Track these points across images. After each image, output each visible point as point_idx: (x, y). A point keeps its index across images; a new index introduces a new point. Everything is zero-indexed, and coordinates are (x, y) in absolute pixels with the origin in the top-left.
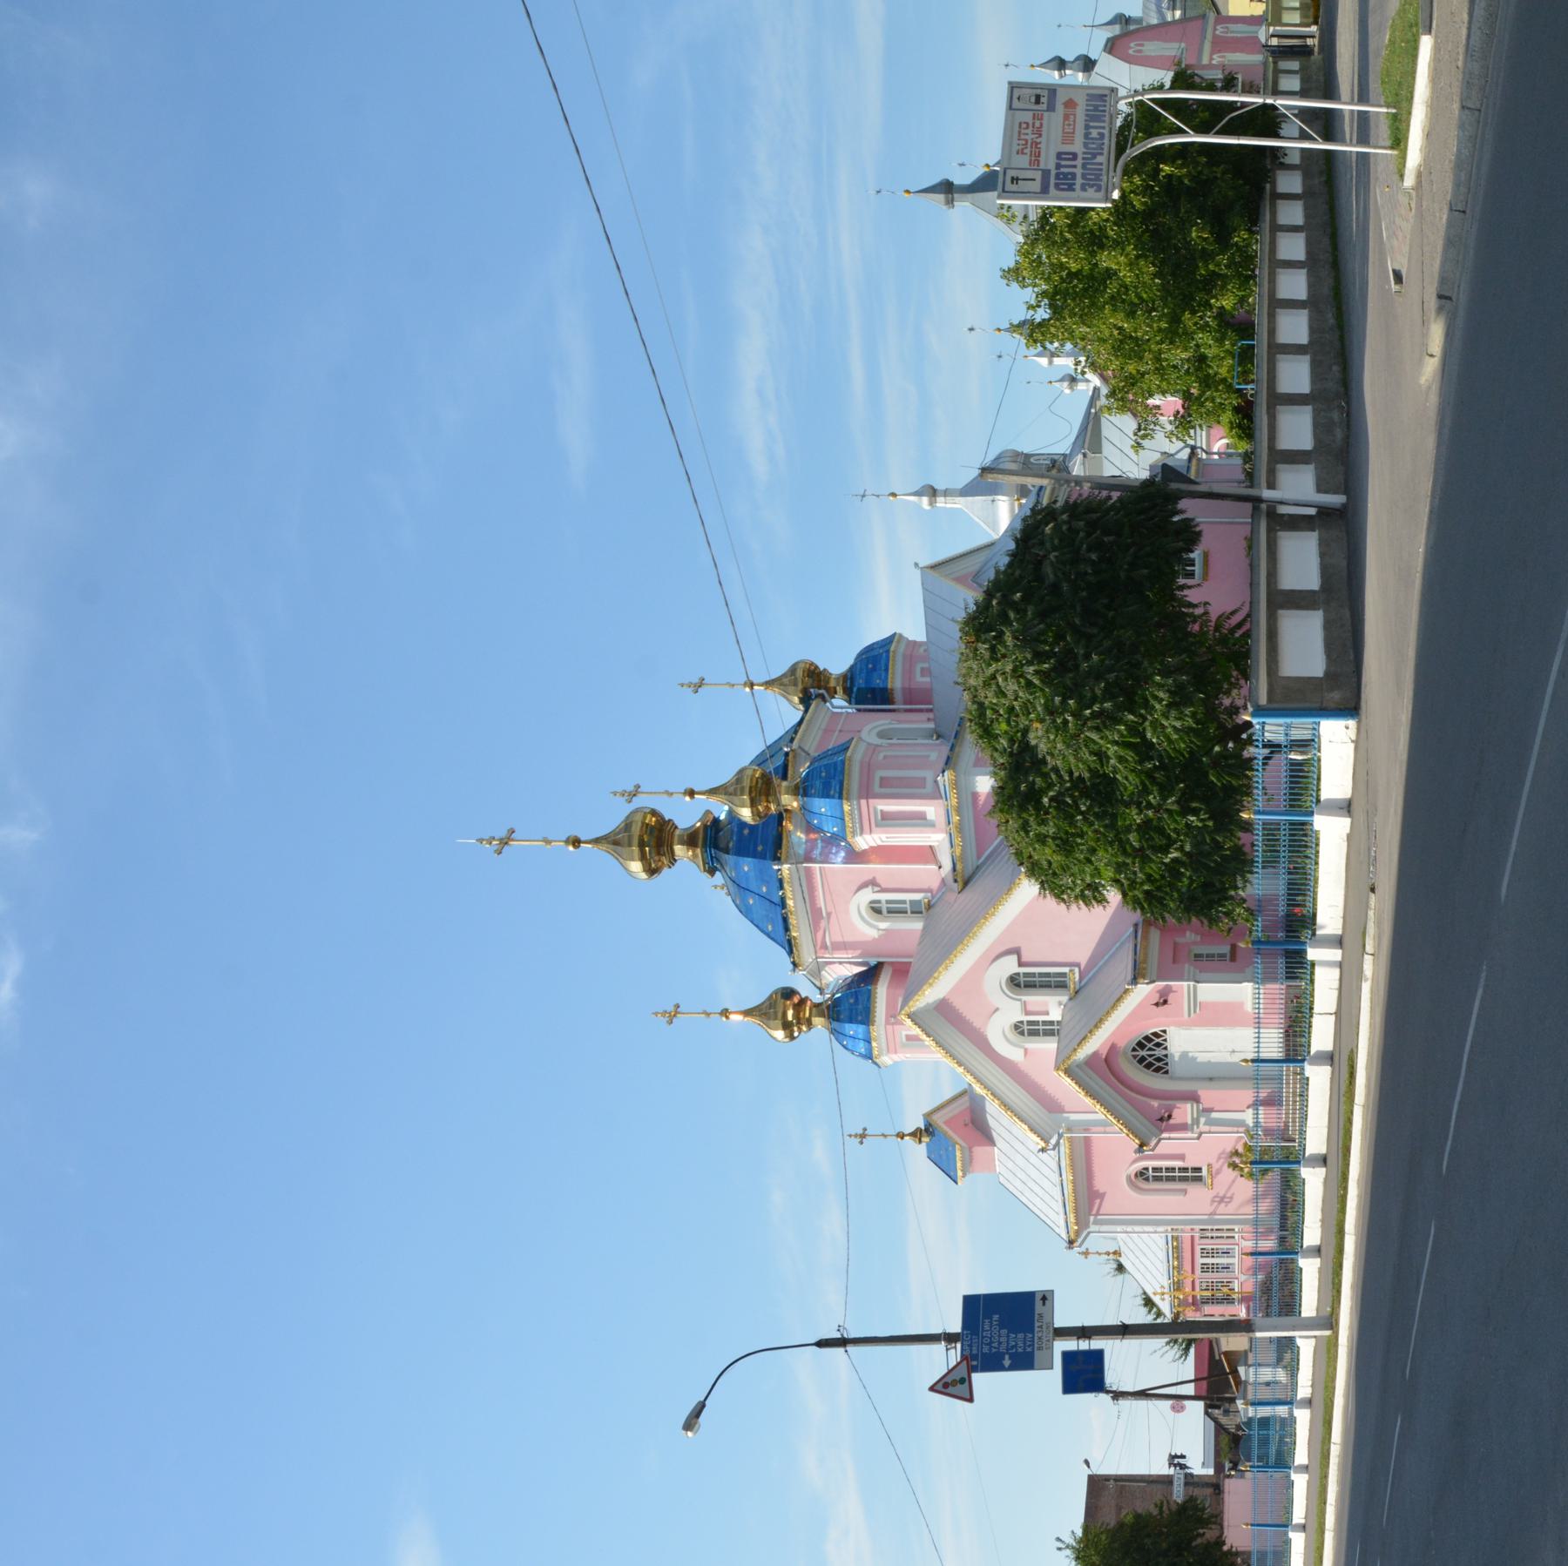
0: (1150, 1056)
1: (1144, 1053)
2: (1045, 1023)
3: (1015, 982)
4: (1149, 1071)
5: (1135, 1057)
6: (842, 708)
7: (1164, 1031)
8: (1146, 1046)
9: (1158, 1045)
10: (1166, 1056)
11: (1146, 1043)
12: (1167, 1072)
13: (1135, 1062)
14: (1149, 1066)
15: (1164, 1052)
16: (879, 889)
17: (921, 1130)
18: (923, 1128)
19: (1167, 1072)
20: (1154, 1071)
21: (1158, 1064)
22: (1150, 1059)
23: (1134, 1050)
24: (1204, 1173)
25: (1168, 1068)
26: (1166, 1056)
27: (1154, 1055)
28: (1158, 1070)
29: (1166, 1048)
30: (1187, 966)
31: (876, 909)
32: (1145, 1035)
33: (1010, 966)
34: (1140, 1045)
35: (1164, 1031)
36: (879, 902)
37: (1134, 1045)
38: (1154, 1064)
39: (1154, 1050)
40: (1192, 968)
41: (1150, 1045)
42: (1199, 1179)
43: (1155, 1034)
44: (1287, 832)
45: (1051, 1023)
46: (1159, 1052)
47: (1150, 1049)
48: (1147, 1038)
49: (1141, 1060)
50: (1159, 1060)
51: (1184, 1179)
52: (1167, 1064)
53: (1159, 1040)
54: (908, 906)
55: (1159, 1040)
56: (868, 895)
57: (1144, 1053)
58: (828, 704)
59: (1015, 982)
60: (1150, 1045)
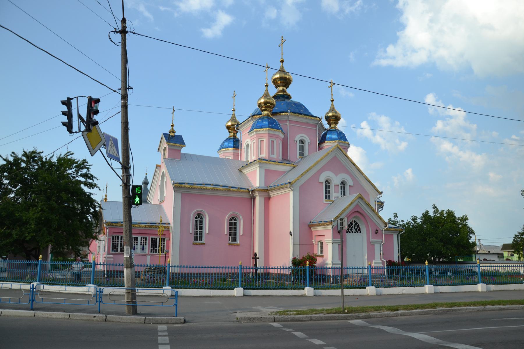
0: (353, 227)
1: (354, 225)
3: (343, 183)
5: (353, 221)
7: (360, 232)
9: (356, 230)
10: (353, 232)
12: (347, 232)
15: (354, 232)
16: (309, 144)
17: (175, 133)
18: (175, 134)
21: (358, 229)
22: (352, 226)
23: (355, 221)
25: (349, 233)
26: (353, 232)
29: (355, 232)
31: (302, 142)
32: (360, 226)
33: (350, 182)
34: (356, 224)
41: (356, 227)
42: (196, 239)
43: (360, 229)
44: (397, 275)
46: (354, 230)
47: (355, 227)
48: (358, 226)
49: (351, 223)
50: (351, 230)
51: (196, 233)
52: (350, 232)
56: (307, 140)
57: (354, 224)
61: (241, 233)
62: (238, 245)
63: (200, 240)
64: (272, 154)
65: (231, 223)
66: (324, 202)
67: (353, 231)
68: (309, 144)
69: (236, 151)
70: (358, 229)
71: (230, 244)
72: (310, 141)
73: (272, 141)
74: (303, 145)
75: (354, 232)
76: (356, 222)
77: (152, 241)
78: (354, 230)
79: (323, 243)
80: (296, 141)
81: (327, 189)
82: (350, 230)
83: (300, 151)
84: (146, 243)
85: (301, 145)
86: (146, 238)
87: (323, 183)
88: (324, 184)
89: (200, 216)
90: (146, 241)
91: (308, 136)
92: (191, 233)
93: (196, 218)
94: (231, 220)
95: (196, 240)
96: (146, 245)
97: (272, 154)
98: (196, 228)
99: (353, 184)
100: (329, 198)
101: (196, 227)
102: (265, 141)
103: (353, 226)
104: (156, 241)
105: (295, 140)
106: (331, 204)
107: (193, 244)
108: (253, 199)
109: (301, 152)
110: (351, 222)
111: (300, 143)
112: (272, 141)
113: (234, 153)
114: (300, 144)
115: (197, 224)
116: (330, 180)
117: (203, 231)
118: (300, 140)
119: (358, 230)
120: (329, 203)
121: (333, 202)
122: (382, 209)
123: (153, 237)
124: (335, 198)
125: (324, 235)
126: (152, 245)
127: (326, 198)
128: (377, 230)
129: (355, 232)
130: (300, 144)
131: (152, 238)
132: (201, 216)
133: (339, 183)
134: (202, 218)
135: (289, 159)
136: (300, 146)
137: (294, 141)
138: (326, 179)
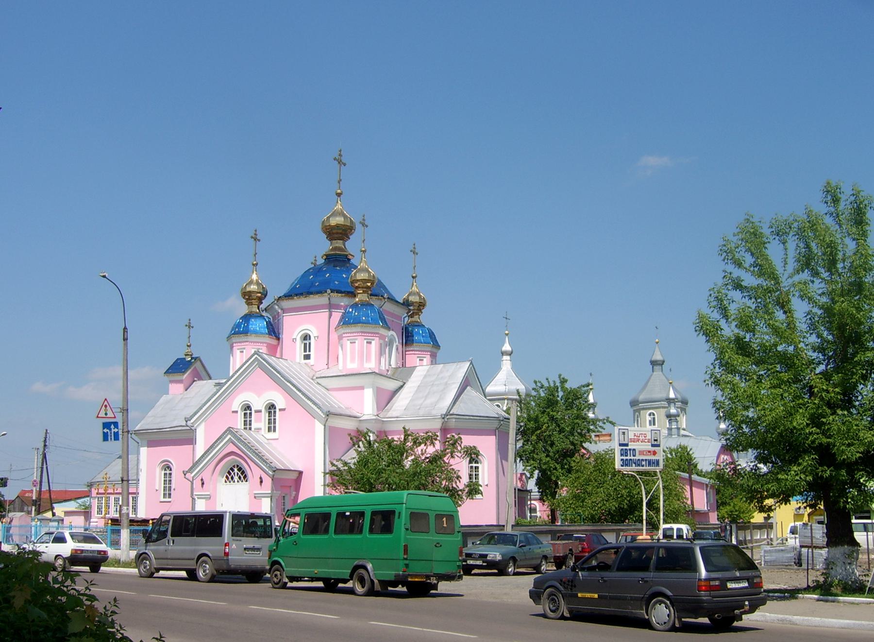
0: (234, 474)
1: (236, 470)
2: (250, 421)
3: (271, 408)
5: (234, 466)
6: (404, 321)
9: (240, 478)
15: (236, 481)
19: (226, 482)
20: (227, 476)
21: (230, 477)
22: (232, 474)
23: (238, 466)
24: (167, 499)
26: (234, 482)
30: (280, 492)
31: (306, 337)
34: (240, 469)
35: (247, 481)
36: (310, 339)
45: (250, 424)
46: (236, 478)
47: (238, 474)
50: (232, 478)
53: (242, 478)
54: (308, 353)
56: (314, 332)
57: (236, 470)
58: (406, 315)
59: (271, 408)
60: (239, 473)
70: (242, 477)
75: (236, 481)
76: (240, 468)
78: (236, 478)
87: (236, 412)
95: (170, 498)
129: (238, 482)
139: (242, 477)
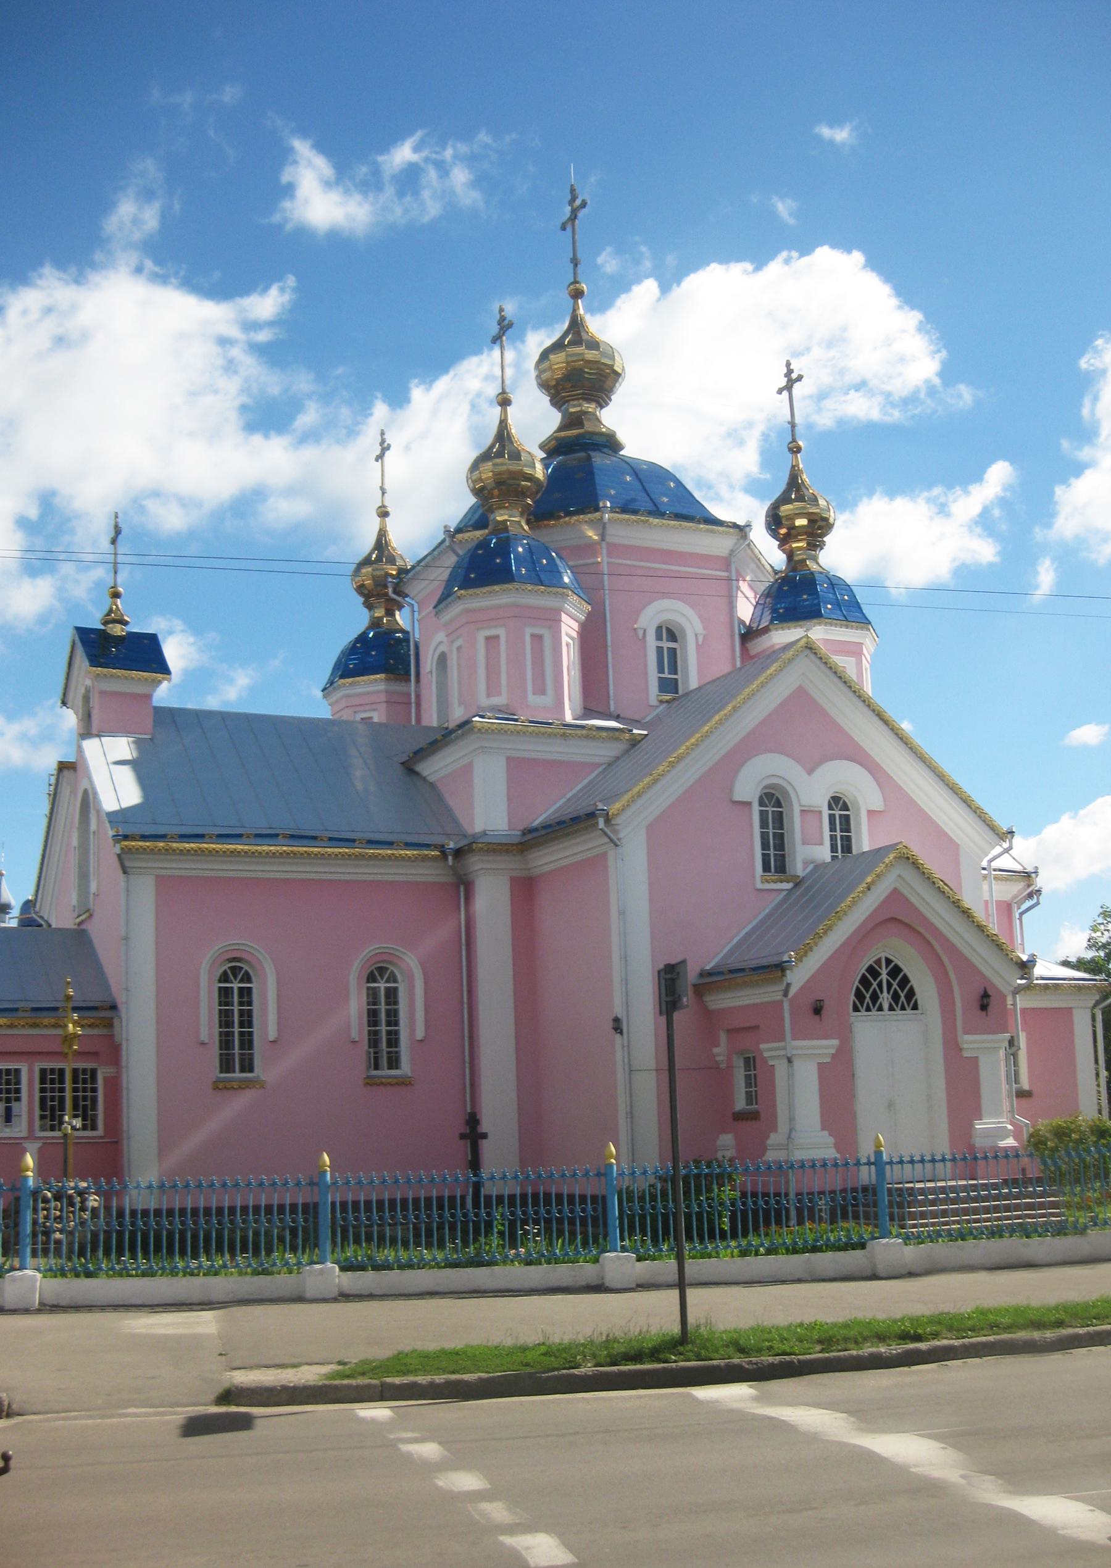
0: (880, 985)
1: (884, 976)
4: (857, 983)
5: (878, 962)
7: (915, 1007)
8: (894, 980)
9: (896, 997)
10: (880, 1009)
11: (897, 981)
12: (856, 1009)
13: (871, 962)
14: (864, 981)
15: (886, 1006)
16: (700, 643)
20: (858, 991)
23: (888, 961)
26: (880, 1009)
27: (882, 992)
28: (859, 995)
29: (891, 1009)
34: (895, 971)
37: (896, 961)
38: (867, 993)
39: (888, 992)
40: (833, 1051)
41: (895, 985)
42: (226, 1065)
43: (911, 994)
46: (885, 998)
47: (889, 985)
48: (905, 981)
49: (873, 971)
50: (875, 998)
51: (226, 1042)
52: (868, 1009)
55: (903, 999)
57: (884, 976)
60: (895, 985)
61: (420, 1034)
62: (404, 1083)
63: (242, 1070)
64: (534, 694)
65: (373, 995)
66: (759, 885)
67: (881, 1004)
68: (700, 643)
69: (399, 687)
70: (902, 995)
71: (370, 1082)
72: (704, 629)
73: (532, 636)
74: (672, 645)
75: (886, 1006)
76: (896, 966)
77: (43, 1081)
78: (885, 998)
79: (754, 1057)
80: (641, 633)
81: (771, 831)
82: (868, 1000)
83: (661, 670)
84: (18, 1091)
85: (667, 645)
86: (17, 1071)
87: (749, 804)
88: (756, 809)
89: (241, 968)
90: (18, 1082)
91: (693, 606)
92: (203, 1044)
93: (224, 978)
94: (371, 978)
96: (18, 1099)
97: (534, 694)
98: (225, 1019)
99: (886, 805)
100: (781, 868)
101: (227, 1016)
102: (503, 640)
103: (881, 982)
104: (62, 1080)
105: (635, 626)
106: (790, 891)
107: (216, 1088)
108: (462, 889)
109: (666, 675)
110: (871, 966)
111: (659, 637)
112: (532, 636)
113: (387, 692)
114: (660, 644)
115: (227, 1004)
116: (786, 793)
117: (256, 1030)
118: (659, 629)
119: (903, 999)
120: (783, 890)
121: (797, 885)
122: (1038, 903)
123: (48, 1065)
124: (806, 863)
125: (757, 1027)
126: (43, 1100)
127: (766, 868)
128: (986, 995)
129: (891, 1009)
130: (660, 644)
131: (43, 1072)
132: (245, 967)
133: (820, 800)
134: (247, 978)
135: (612, 709)
136: (660, 650)
137: (635, 629)
138: (765, 787)
139: (902, 995)
